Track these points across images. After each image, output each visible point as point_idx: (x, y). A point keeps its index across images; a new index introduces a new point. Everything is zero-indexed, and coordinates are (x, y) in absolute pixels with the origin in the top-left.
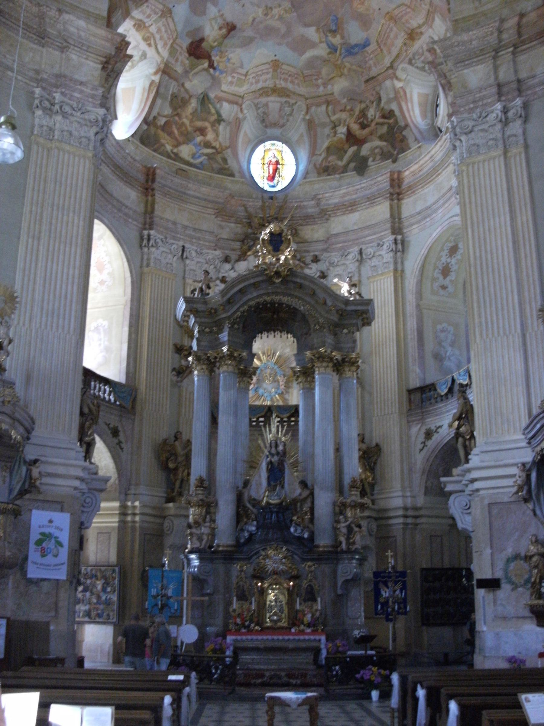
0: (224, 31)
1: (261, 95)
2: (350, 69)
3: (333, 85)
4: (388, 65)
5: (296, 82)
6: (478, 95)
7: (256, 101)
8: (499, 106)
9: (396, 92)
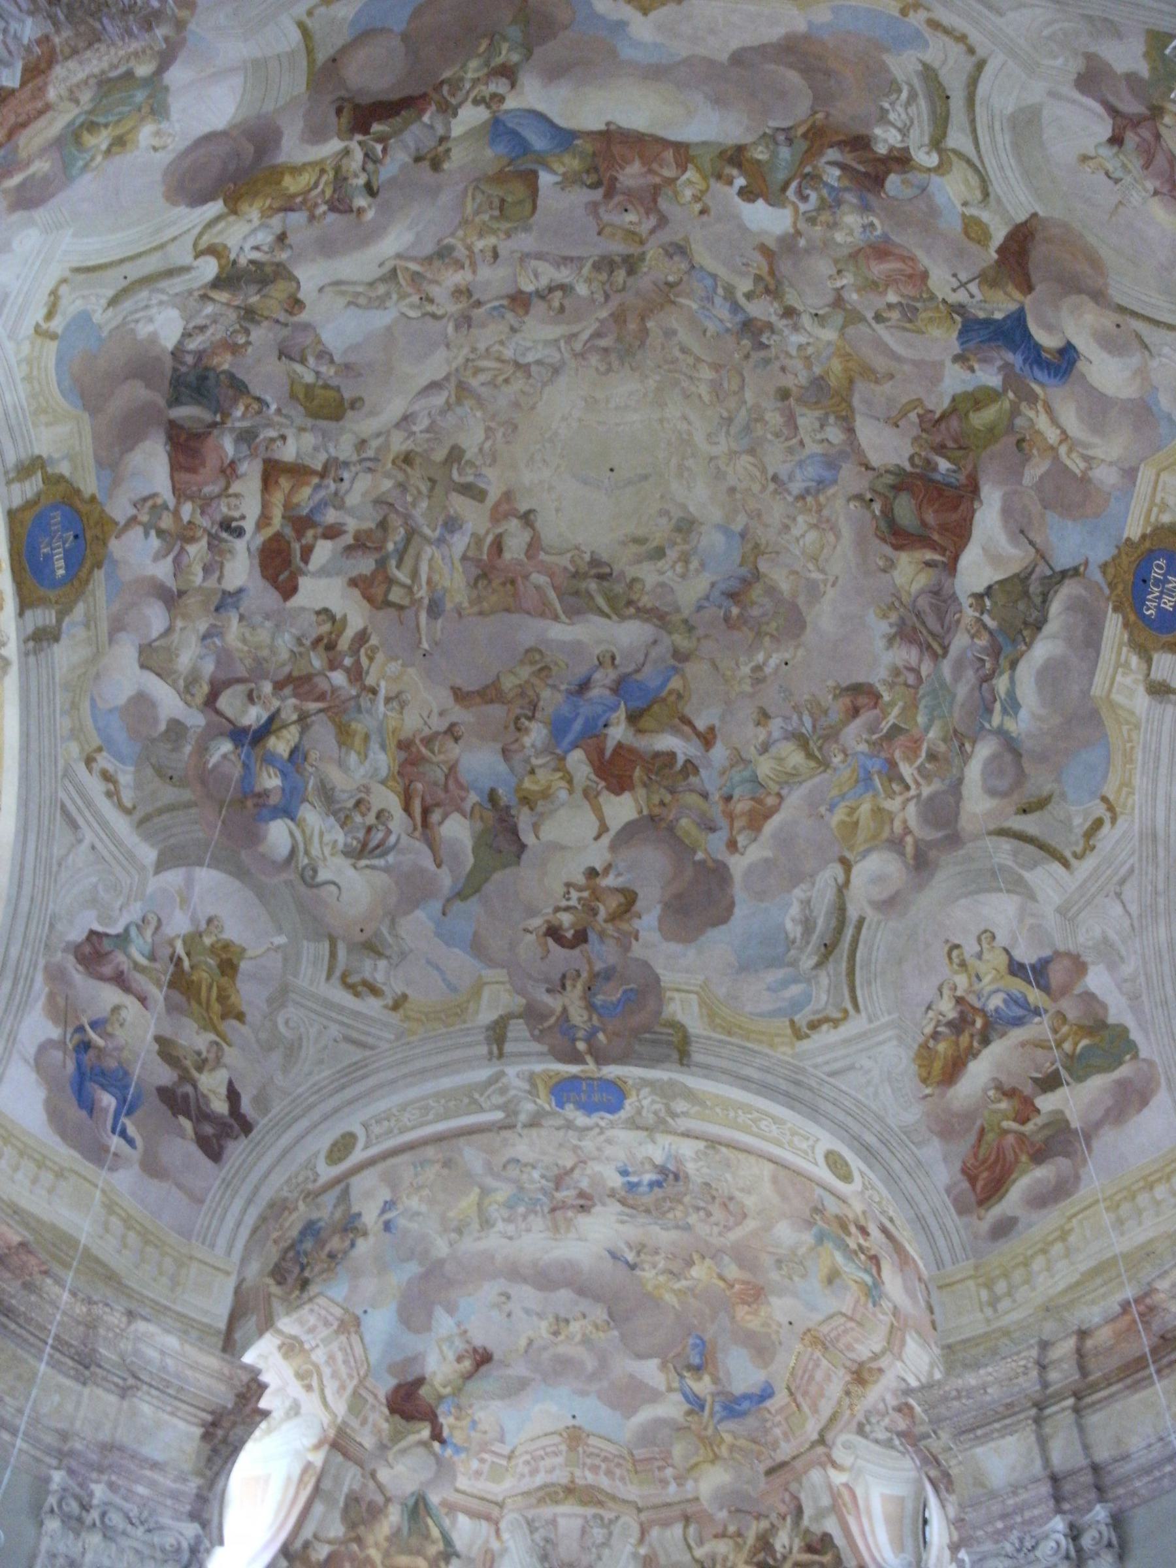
0: (467, 1364)
1: (541, 1501)
2: (732, 1448)
3: (696, 1480)
4: (815, 1436)
5: (618, 1472)
6: (1011, 1502)
7: (530, 1514)
8: (1058, 1524)
9: (835, 1495)
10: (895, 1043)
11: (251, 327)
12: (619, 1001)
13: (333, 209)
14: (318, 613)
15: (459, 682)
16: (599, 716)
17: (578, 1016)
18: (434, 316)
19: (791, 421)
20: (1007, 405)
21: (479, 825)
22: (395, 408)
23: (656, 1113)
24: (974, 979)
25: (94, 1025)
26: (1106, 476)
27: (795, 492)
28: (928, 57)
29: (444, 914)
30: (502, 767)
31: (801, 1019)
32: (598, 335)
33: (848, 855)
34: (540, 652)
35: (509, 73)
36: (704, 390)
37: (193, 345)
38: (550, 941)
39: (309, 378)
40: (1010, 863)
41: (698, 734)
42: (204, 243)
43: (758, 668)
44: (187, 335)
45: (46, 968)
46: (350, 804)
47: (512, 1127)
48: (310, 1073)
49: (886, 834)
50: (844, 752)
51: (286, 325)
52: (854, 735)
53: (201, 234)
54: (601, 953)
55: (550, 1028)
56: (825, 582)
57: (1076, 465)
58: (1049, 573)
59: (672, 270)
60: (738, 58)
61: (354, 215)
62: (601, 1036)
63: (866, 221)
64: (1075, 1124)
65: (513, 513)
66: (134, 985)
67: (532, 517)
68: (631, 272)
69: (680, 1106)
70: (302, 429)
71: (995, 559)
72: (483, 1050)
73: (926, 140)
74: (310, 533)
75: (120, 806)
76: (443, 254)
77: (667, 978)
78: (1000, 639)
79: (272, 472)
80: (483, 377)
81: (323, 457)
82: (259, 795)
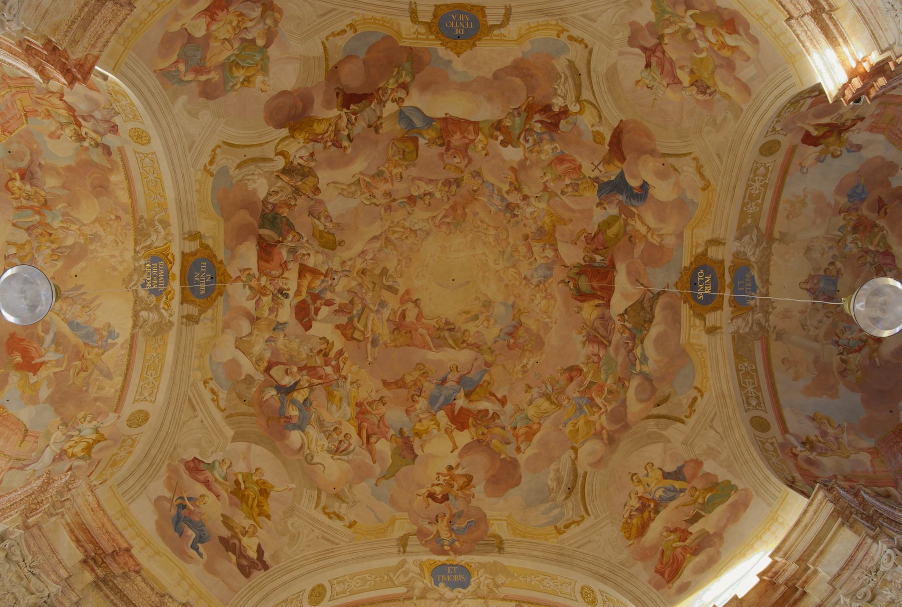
10: (611, 525)
11: (297, 197)
12: (466, 527)
13: (334, 145)
14: (321, 339)
15: (385, 378)
16: (451, 395)
17: (445, 534)
18: (375, 204)
19: (530, 249)
20: (622, 222)
21: (395, 445)
22: (358, 247)
23: (488, 587)
24: (646, 486)
25: (190, 499)
26: (670, 241)
27: (535, 283)
28: (569, 58)
29: (376, 485)
30: (406, 419)
31: (560, 525)
32: (445, 216)
33: (575, 445)
34: (424, 365)
35: (404, 86)
36: (491, 239)
37: (272, 200)
38: (429, 499)
39: (321, 228)
40: (656, 429)
41: (499, 400)
42: (280, 148)
43: (524, 366)
44: (269, 194)
45: (169, 465)
46: (333, 428)
47: (410, 598)
48: (303, 550)
49: (593, 432)
50: (568, 398)
51: (312, 199)
52: (572, 390)
53: (278, 144)
54: (456, 505)
55: (431, 540)
56: (552, 322)
57: (655, 241)
58: (652, 296)
59: (474, 184)
60: (496, 76)
61: (342, 149)
62: (457, 543)
63: (553, 146)
64: (711, 532)
65: (410, 300)
66: (214, 488)
67: (418, 302)
68: (458, 186)
69: (501, 579)
70: (317, 252)
71: (626, 296)
72: (396, 549)
73: (574, 99)
74: (319, 302)
75: (218, 406)
76: (379, 174)
77: (489, 514)
78: (634, 331)
79: (303, 270)
80: (396, 235)
81: (326, 267)
82: (287, 418)
